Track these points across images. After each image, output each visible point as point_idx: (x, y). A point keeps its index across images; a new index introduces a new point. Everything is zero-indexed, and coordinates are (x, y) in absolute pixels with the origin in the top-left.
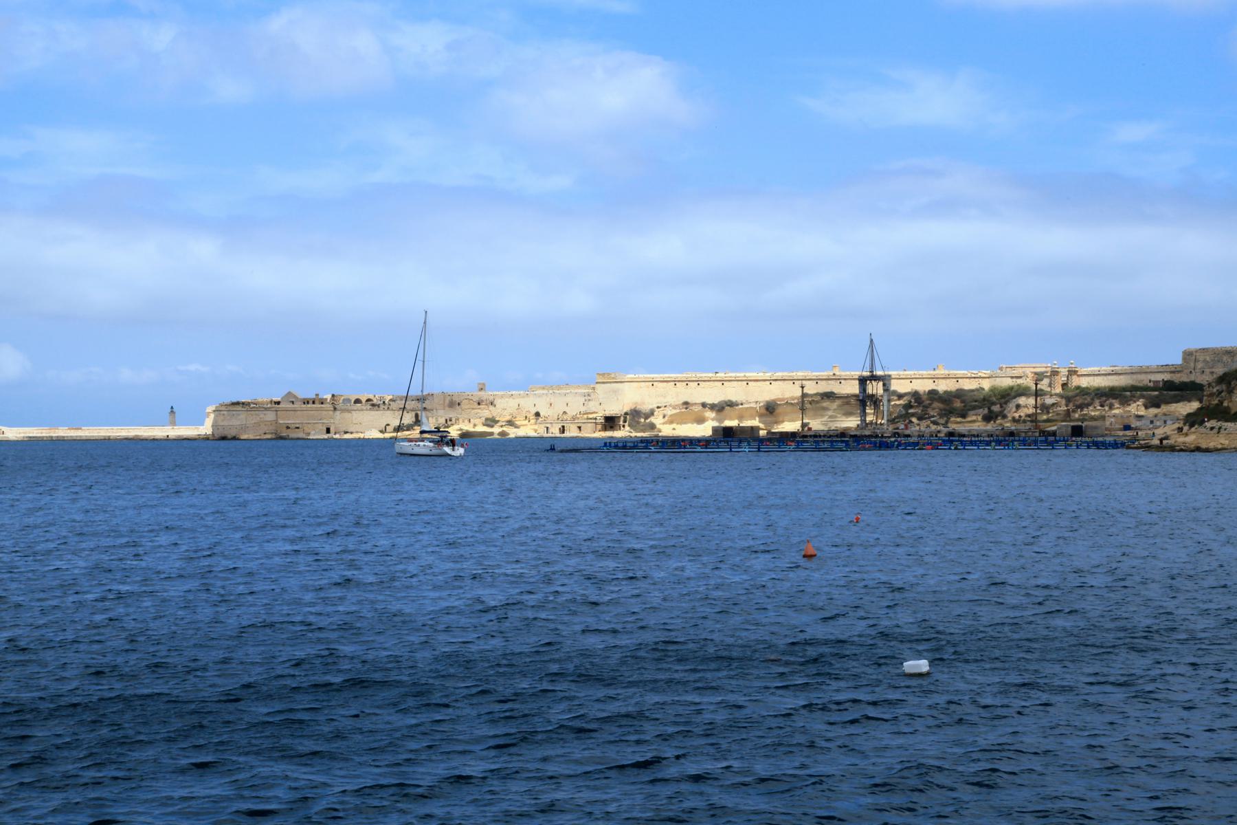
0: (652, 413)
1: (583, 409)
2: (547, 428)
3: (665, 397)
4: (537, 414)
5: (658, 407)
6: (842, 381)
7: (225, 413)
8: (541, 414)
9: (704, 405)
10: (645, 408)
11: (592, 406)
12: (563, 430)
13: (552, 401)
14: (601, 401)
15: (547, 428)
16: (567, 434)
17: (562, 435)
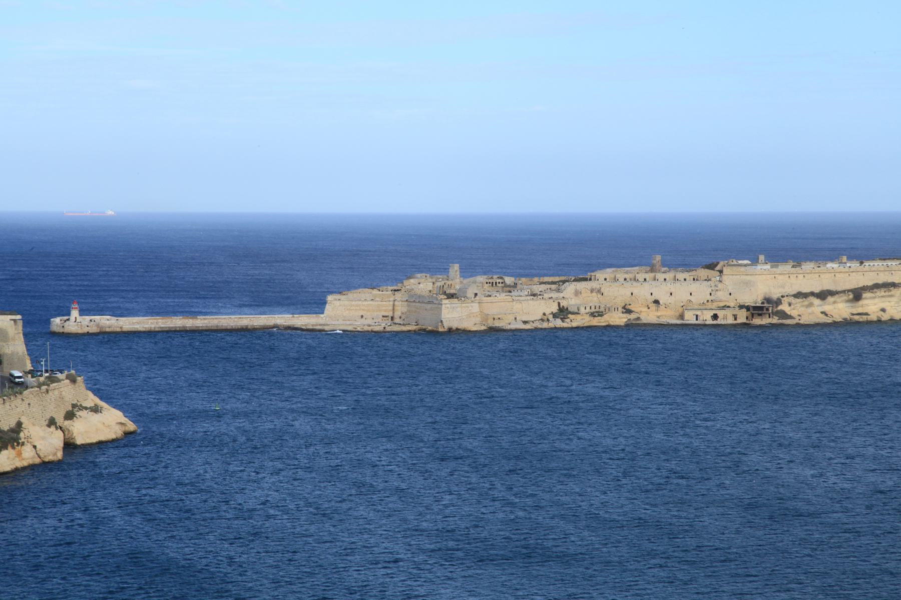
0: (778, 302)
1: (710, 298)
2: (697, 316)
3: (784, 288)
4: (656, 302)
5: (783, 297)
6: (893, 272)
7: (448, 305)
8: (661, 302)
9: (813, 294)
10: (775, 297)
12: (715, 317)
13: (672, 290)
14: (731, 291)
15: (697, 316)
16: (719, 321)
17: (715, 322)
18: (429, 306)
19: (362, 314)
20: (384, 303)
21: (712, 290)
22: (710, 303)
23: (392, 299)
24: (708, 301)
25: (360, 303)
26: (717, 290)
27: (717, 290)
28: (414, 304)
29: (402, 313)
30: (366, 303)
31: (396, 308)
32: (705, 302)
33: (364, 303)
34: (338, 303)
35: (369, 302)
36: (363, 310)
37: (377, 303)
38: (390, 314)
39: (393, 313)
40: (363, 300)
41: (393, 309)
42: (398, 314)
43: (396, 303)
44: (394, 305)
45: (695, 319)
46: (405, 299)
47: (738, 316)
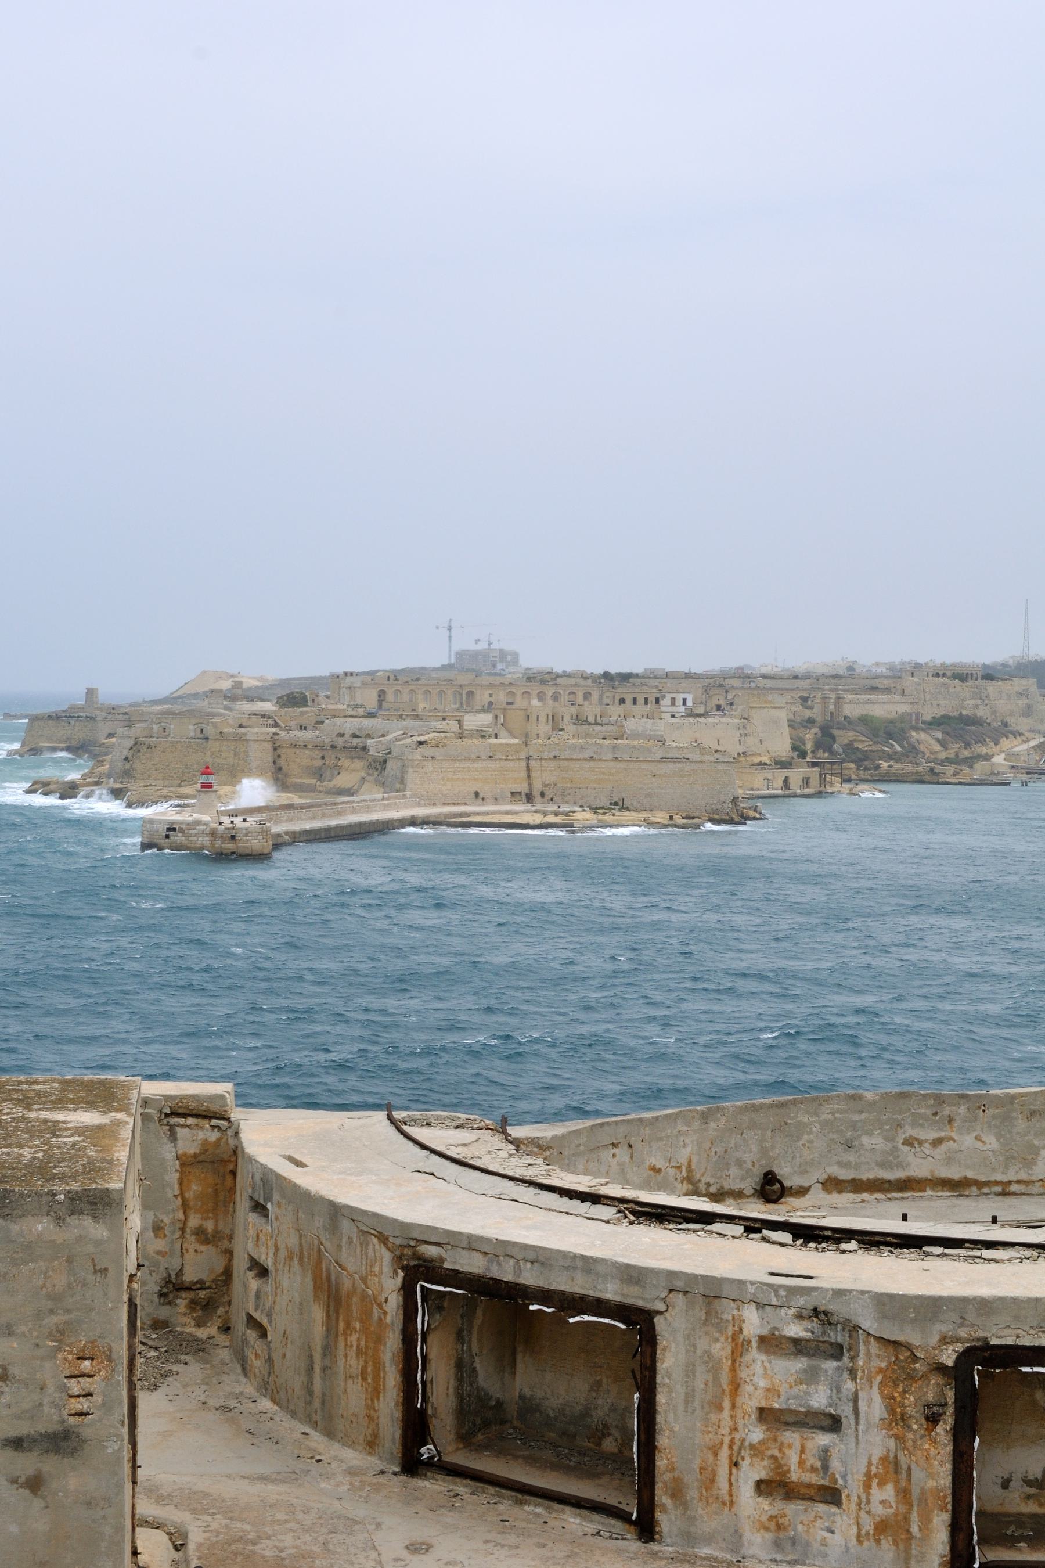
11: (751, 742)
18: (671, 767)
19: (475, 789)
20: (511, 764)
21: (741, 735)
22: (742, 759)
23: (523, 755)
24: (739, 754)
25: (467, 764)
26: (746, 735)
27: (746, 735)
28: (592, 764)
29: (546, 786)
30: (479, 765)
31: (534, 774)
32: (736, 756)
33: (476, 765)
34: (429, 765)
35: (484, 764)
36: (475, 779)
37: (498, 764)
38: (524, 788)
39: (530, 785)
40: (473, 757)
41: (529, 776)
42: (537, 787)
43: (532, 763)
44: (528, 768)
45: (766, 788)
46: (551, 755)
47: (811, 780)
